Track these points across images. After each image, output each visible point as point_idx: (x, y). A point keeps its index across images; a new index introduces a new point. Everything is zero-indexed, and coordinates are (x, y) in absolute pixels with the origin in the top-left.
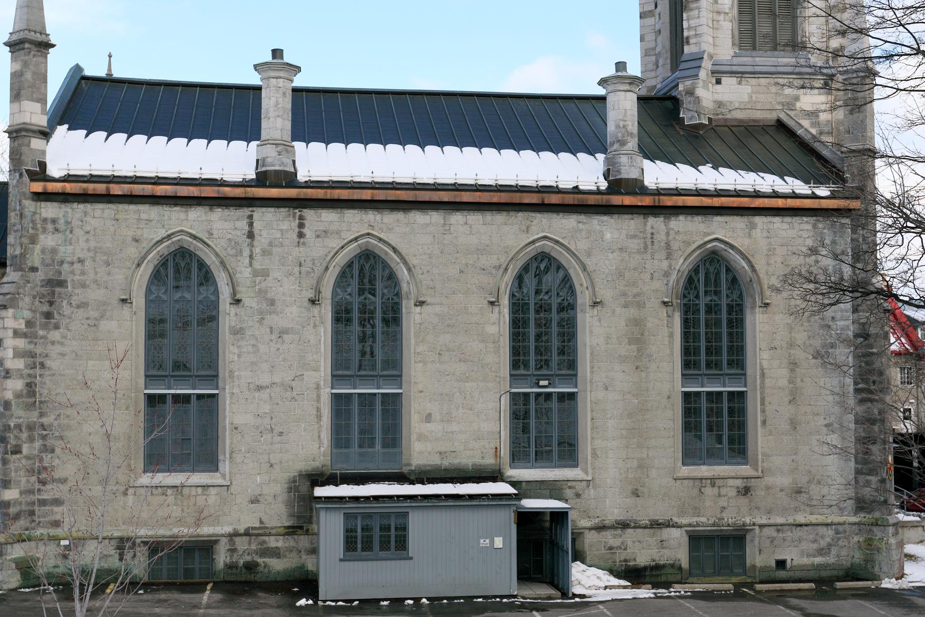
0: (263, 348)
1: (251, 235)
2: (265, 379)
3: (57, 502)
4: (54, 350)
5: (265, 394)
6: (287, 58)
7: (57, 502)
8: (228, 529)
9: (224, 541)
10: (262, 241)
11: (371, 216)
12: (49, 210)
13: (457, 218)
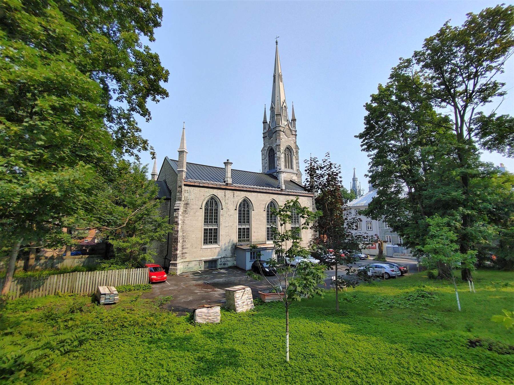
0: (227, 219)
1: (225, 196)
2: (227, 225)
3: (186, 253)
4: (186, 219)
5: (227, 228)
6: (230, 161)
7: (186, 253)
8: (220, 257)
9: (219, 260)
10: (227, 197)
11: (245, 193)
12: (187, 188)
13: (259, 194)
